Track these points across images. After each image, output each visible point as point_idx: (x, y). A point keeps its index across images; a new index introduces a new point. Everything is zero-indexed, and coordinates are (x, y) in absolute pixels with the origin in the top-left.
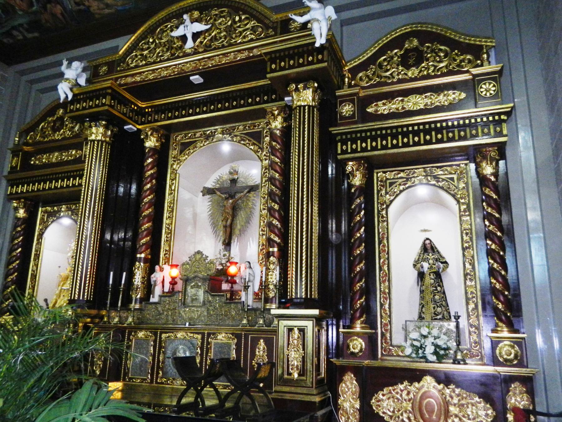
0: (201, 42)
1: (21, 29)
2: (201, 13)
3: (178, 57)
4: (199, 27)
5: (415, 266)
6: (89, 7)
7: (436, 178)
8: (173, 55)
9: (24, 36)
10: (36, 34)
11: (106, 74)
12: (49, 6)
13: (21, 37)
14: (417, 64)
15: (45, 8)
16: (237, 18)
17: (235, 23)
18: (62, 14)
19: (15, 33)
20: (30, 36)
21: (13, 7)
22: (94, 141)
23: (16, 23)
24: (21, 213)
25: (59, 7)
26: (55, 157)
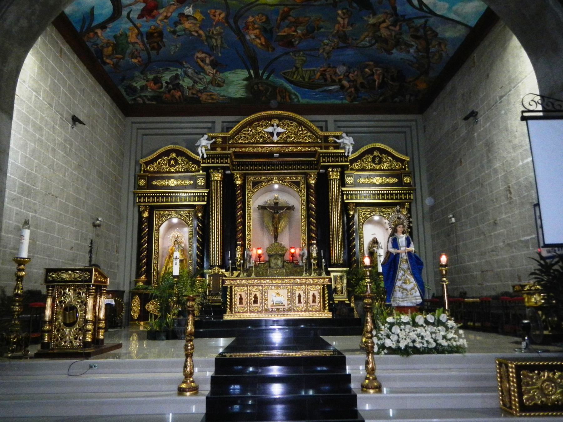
0: (281, 138)
1: (144, 98)
2: (280, 121)
3: (268, 143)
4: (280, 130)
5: (369, 249)
6: (200, 97)
7: (382, 212)
8: (265, 141)
9: (144, 102)
10: (154, 103)
11: (220, 144)
12: (173, 91)
13: (141, 102)
14: (379, 164)
15: (169, 91)
16: (300, 129)
17: (300, 131)
18: (179, 97)
19: (139, 99)
20: (150, 102)
21: (147, 87)
22: (217, 181)
23: (142, 94)
24: (146, 215)
25: (179, 94)
26: (173, 183)
